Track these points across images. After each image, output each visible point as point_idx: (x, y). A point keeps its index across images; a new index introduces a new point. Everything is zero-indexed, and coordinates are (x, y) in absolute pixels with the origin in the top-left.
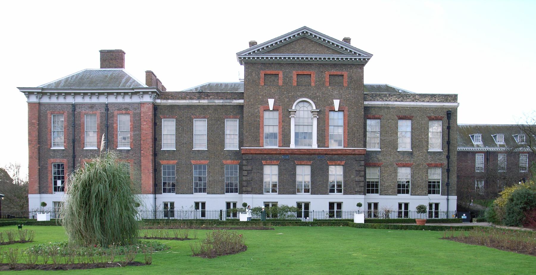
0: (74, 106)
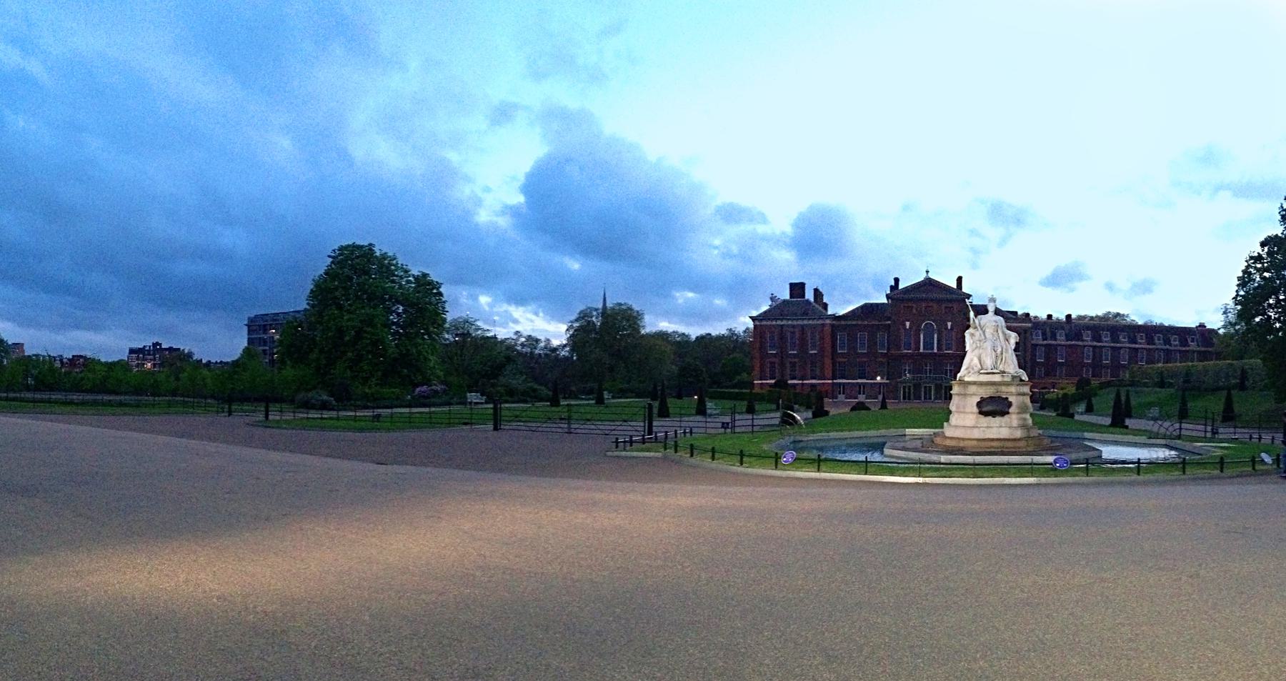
0: (782, 326)
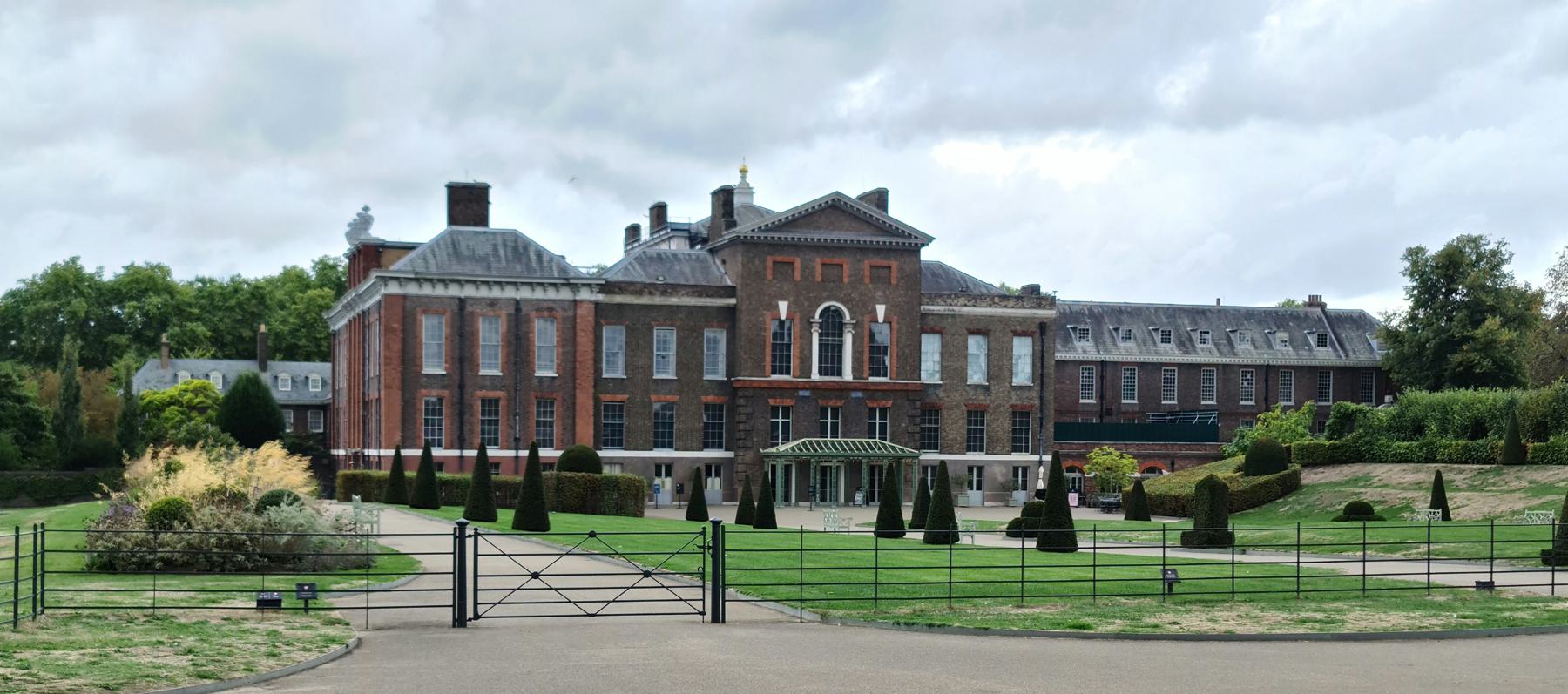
0: (462, 302)
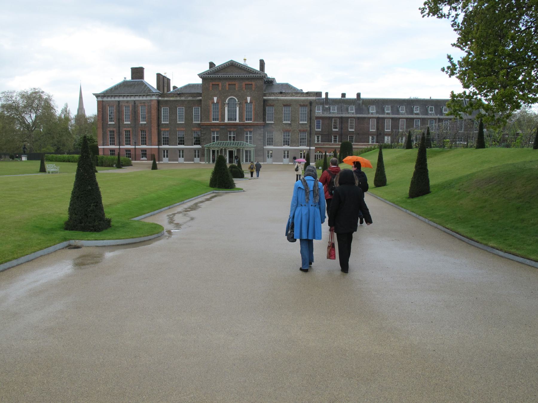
0: (119, 102)
